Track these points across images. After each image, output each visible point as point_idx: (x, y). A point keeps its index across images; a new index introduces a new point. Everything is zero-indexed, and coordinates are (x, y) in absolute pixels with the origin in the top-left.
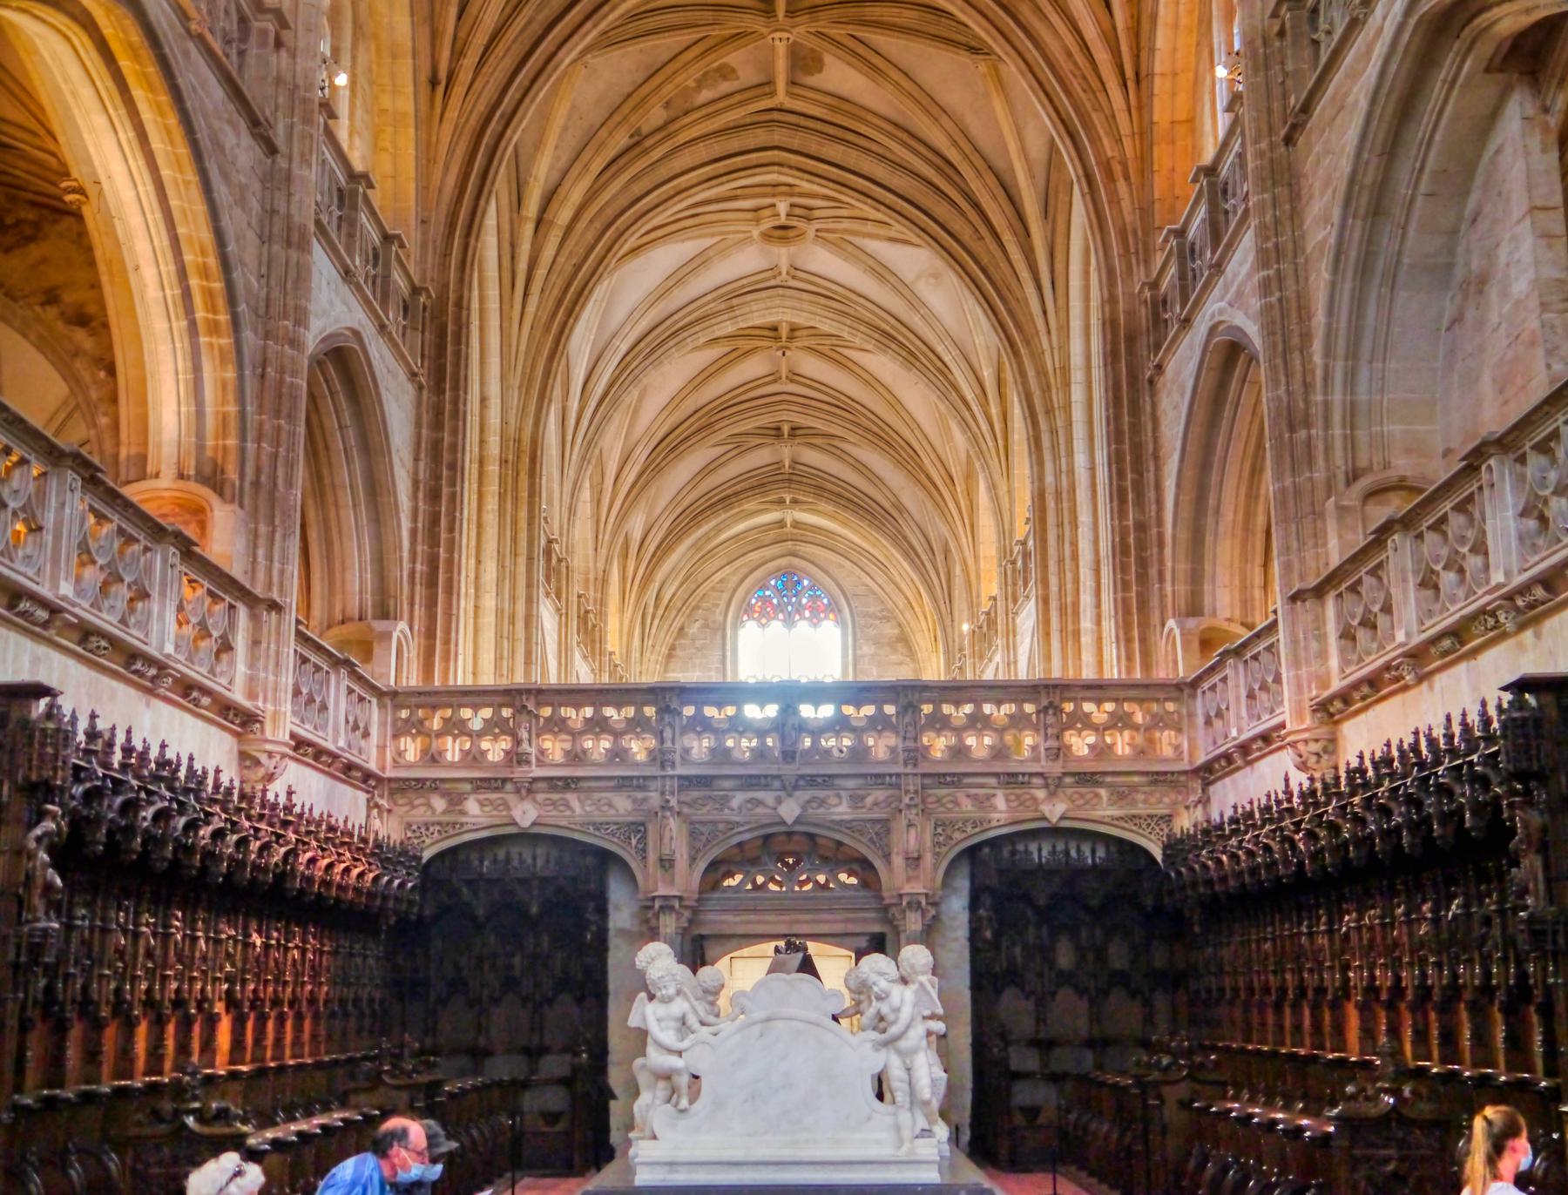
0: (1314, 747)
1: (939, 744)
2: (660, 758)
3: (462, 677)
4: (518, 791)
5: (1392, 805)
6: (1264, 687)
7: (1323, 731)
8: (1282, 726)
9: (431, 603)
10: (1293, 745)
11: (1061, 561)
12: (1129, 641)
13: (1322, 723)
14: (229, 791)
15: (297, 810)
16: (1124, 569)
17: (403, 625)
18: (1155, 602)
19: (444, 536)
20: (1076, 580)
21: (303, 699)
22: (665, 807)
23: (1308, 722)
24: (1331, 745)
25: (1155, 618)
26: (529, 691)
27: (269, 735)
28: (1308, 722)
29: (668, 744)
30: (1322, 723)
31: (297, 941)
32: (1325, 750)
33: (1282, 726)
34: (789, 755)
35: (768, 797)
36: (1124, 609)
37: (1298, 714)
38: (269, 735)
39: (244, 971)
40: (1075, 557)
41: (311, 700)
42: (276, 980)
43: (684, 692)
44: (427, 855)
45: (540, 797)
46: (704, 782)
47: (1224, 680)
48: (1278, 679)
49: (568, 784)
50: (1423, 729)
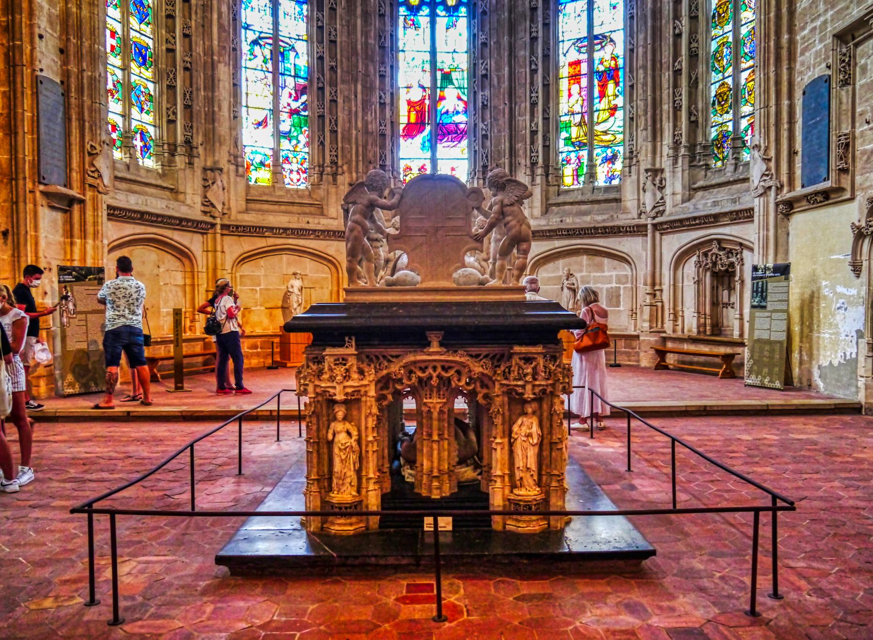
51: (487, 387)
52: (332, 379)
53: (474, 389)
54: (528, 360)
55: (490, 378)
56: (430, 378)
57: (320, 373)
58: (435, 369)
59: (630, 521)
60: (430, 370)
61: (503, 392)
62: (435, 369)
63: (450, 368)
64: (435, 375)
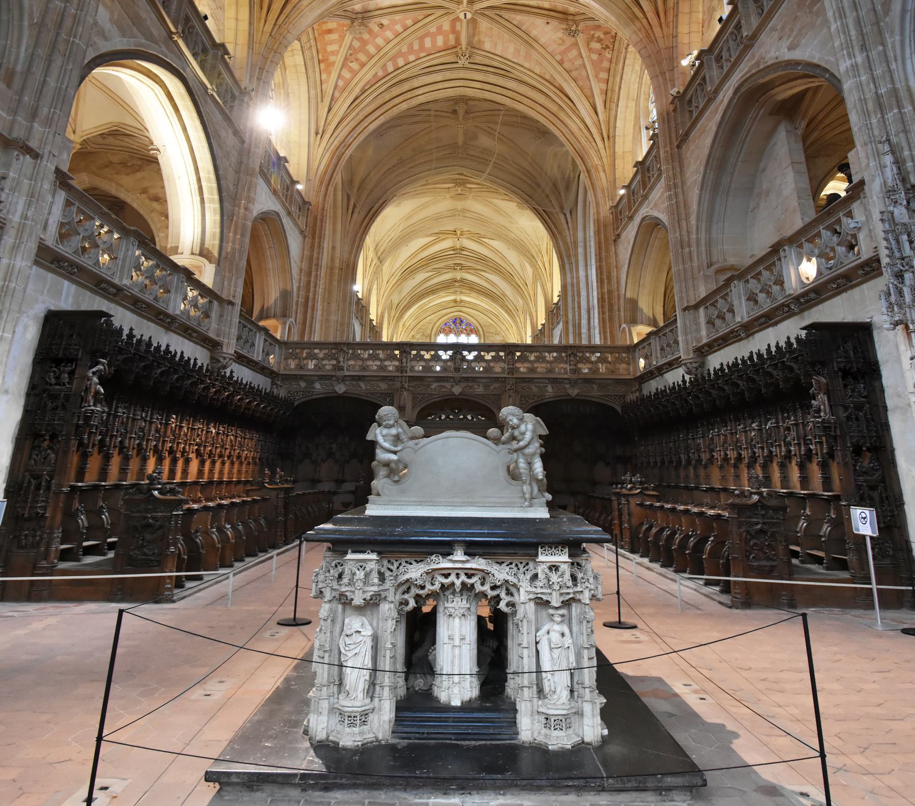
0: (694, 365)
1: (523, 368)
2: (400, 369)
3: (316, 338)
4: (338, 380)
5: (740, 382)
6: (669, 345)
7: (699, 360)
8: (680, 357)
9: (306, 313)
10: (685, 364)
11: (574, 308)
12: (605, 332)
13: (698, 356)
14: (201, 367)
15: (235, 379)
16: (603, 307)
17: (292, 320)
18: (616, 319)
19: (312, 289)
20: (580, 315)
21: (242, 341)
22: (403, 387)
23: (692, 356)
24: (703, 364)
25: (617, 324)
26: (344, 344)
27: (225, 350)
28: (692, 356)
29: (404, 364)
30: (698, 356)
31: (233, 433)
32: (700, 366)
33: (680, 357)
34: (457, 370)
35: (448, 385)
36: (602, 321)
37: (687, 352)
38: (225, 350)
39: (206, 442)
40: (579, 307)
41: (247, 341)
42: (222, 447)
43: (412, 346)
44: (296, 403)
45: (347, 383)
46: (420, 379)
47: (649, 344)
48: (676, 342)
49: (360, 378)
50: (755, 351)
51: (512, 595)
52: (351, 583)
53: (498, 595)
54: (554, 568)
55: (515, 585)
56: (453, 584)
57: (340, 576)
58: (458, 575)
59: (745, 762)
60: (452, 578)
61: (530, 600)
62: (458, 575)
63: (473, 575)
64: (458, 583)
